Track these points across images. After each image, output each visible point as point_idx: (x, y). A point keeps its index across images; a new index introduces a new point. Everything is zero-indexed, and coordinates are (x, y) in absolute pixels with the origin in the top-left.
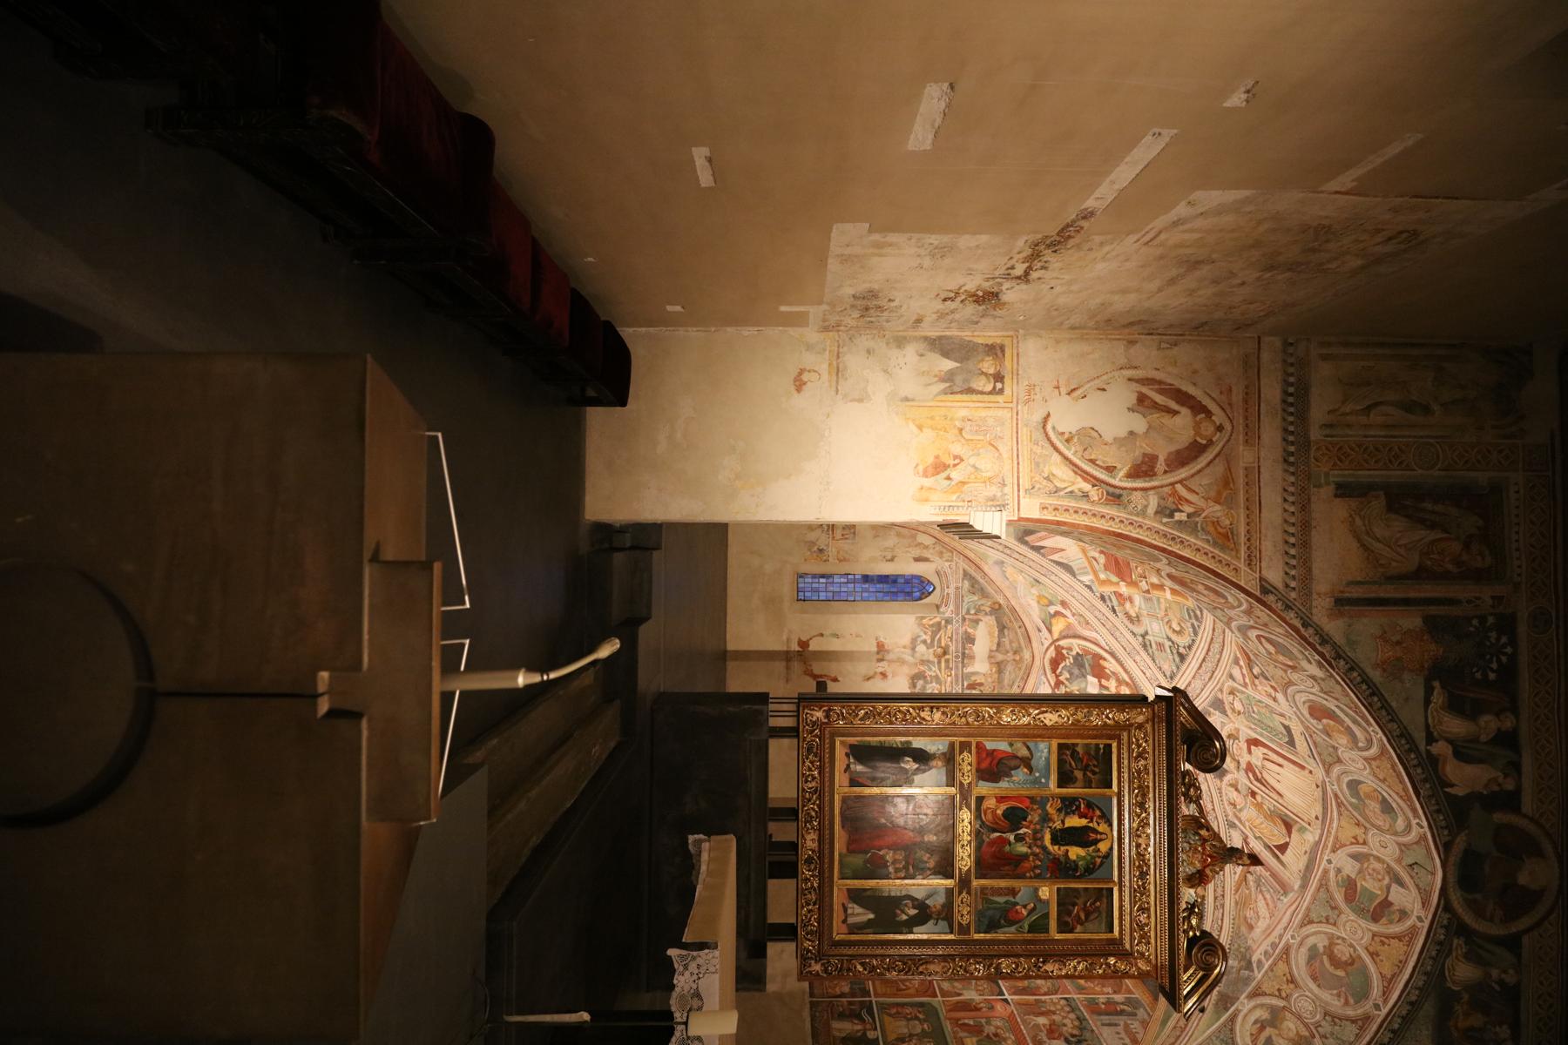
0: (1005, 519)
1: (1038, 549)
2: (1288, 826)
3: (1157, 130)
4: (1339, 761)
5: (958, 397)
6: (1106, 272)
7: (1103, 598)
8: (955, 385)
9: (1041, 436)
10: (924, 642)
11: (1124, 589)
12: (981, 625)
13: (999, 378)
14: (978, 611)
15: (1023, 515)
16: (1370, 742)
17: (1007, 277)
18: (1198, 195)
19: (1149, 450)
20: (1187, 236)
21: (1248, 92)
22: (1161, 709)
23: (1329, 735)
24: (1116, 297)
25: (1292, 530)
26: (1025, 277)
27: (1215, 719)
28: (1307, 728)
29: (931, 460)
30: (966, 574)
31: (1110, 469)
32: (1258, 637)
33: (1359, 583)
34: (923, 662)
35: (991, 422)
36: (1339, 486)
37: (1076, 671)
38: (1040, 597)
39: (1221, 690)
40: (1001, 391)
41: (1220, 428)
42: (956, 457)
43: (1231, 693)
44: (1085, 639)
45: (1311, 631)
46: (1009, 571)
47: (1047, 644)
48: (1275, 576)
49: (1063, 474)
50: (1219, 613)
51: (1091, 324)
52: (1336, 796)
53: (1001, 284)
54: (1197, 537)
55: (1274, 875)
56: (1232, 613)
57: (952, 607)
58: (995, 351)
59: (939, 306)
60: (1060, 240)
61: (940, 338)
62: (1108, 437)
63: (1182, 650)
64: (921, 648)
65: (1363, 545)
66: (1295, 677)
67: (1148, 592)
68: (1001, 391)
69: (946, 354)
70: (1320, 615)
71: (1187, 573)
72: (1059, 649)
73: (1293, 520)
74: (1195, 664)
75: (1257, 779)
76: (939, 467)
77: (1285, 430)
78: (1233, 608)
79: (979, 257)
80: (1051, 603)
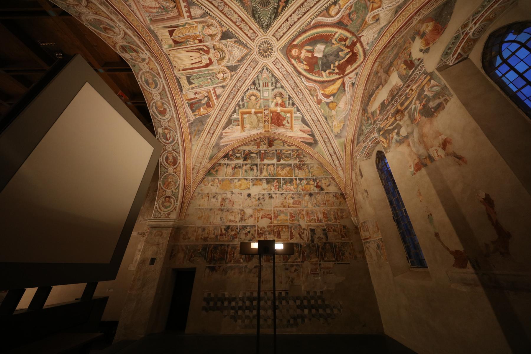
1: (312, 135)
2: (176, 42)
4: (160, 94)
7: (293, 104)
10: (398, 134)
11: (279, 109)
12: (373, 109)
14: (369, 119)
16: (152, 107)
30: (358, 143)
37: (331, 58)
44: (315, 81)
46: (337, 130)
47: (352, 75)
52: (160, 77)
55: (163, 20)
57: (373, 136)
63: (253, 87)
66: (167, 125)
67: (265, 110)
75: (202, 49)
80: (328, 104)
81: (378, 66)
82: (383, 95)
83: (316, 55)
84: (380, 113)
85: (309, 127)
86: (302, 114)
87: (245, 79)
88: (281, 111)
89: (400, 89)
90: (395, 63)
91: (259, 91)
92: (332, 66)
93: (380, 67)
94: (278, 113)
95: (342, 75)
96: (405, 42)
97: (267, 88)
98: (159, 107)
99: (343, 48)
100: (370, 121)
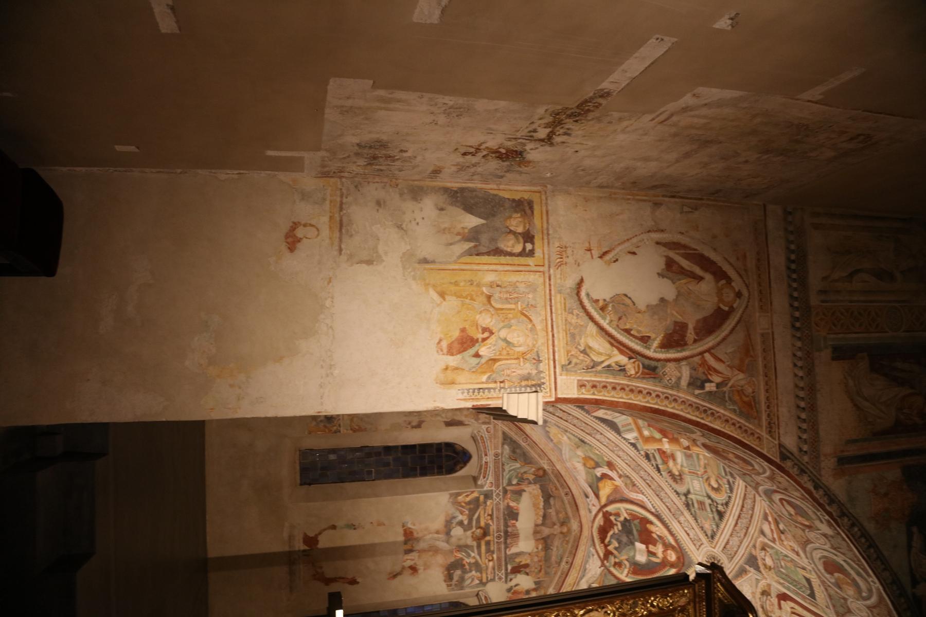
0: (541, 401)
3: (658, 36)
5: (485, 259)
6: (626, 142)
7: (647, 456)
8: (482, 245)
9: (572, 303)
10: (461, 523)
11: (666, 446)
12: (525, 497)
13: (528, 237)
14: (521, 480)
15: (559, 396)
17: (531, 138)
18: (700, 90)
19: (679, 318)
20: (696, 120)
21: (732, 19)
22: (701, 589)
23: (840, 588)
24: (639, 164)
25: (802, 394)
26: (549, 140)
27: (747, 587)
28: (823, 582)
29: (456, 334)
30: (506, 438)
31: (645, 340)
32: (781, 500)
33: (854, 441)
34: (461, 548)
35: (522, 288)
36: (835, 349)
37: (624, 539)
38: (586, 459)
39: (754, 546)
40: (531, 253)
41: (739, 295)
42: (485, 330)
43: (763, 549)
44: (632, 502)
45: (821, 492)
46: (553, 431)
48: (790, 442)
49: (599, 345)
50: (748, 478)
51: (618, 184)
53: (524, 145)
54: (725, 409)
56: (759, 479)
57: (491, 479)
58: (523, 207)
59: (461, 160)
60: (581, 112)
61: (462, 190)
62: (641, 306)
63: (720, 508)
64: (457, 531)
65: (855, 405)
66: (811, 535)
67: (688, 448)
68: (531, 253)
69: (469, 209)
70: (828, 479)
71: (717, 441)
72: (606, 515)
73: (802, 384)
74: (732, 522)
76: (465, 343)
77: (791, 296)
78: (759, 474)
79: (498, 121)
80: (597, 465)
81: (569, 531)
82: (526, 522)
83: (643, 547)
84: (508, 507)
85: (597, 418)
86: (625, 439)
87: (736, 528)
88: (660, 440)
89: (506, 548)
90: (542, 554)
91: (709, 497)
92: (620, 528)
93: (565, 530)
94: (665, 436)
95: (605, 510)
96: (547, 573)
97: (701, 498)
98: (847, 584)
99: (615, 552)
100: (514, 482)
